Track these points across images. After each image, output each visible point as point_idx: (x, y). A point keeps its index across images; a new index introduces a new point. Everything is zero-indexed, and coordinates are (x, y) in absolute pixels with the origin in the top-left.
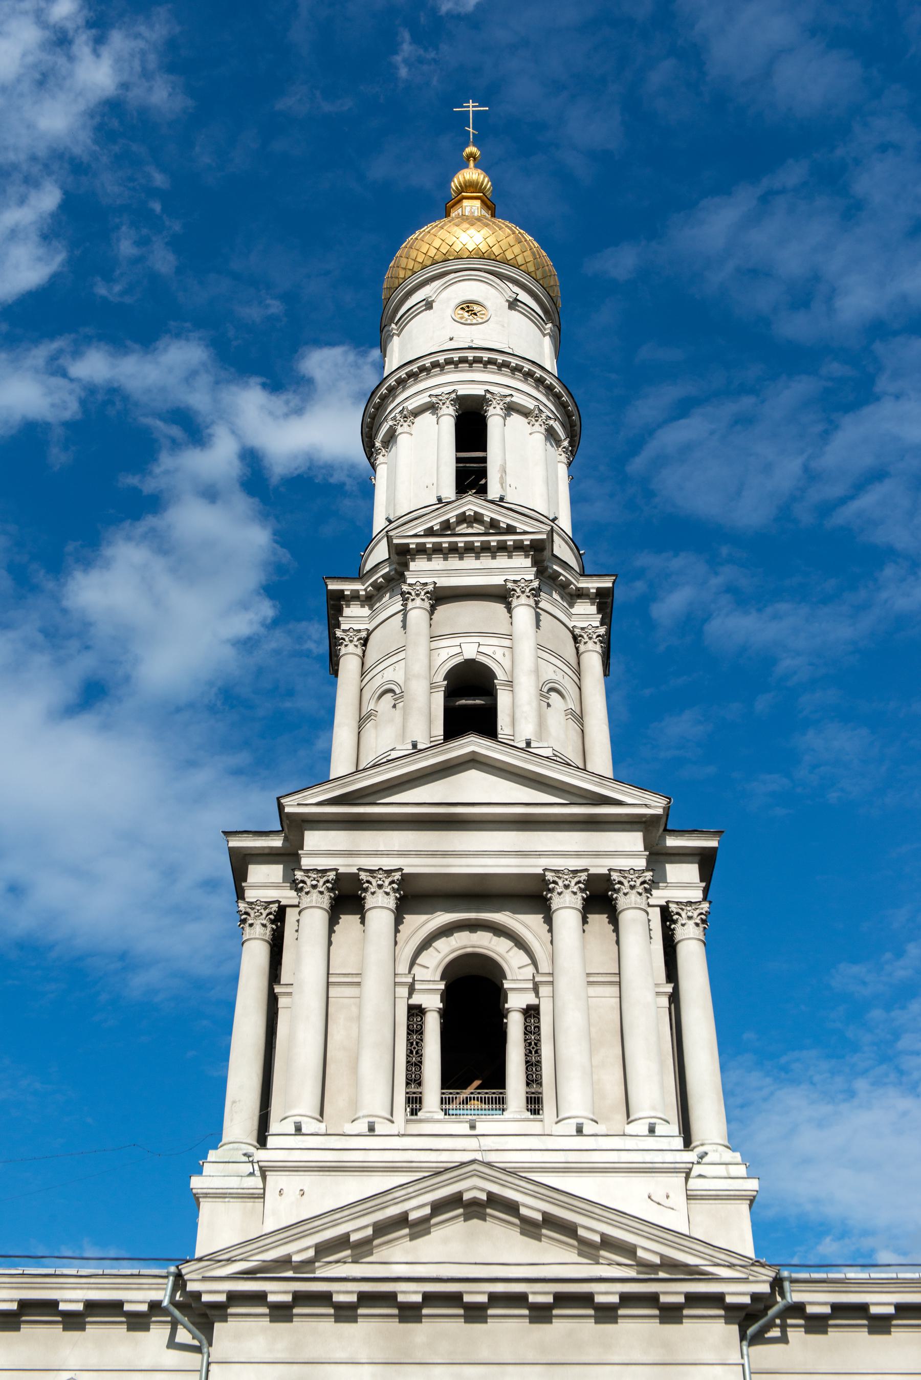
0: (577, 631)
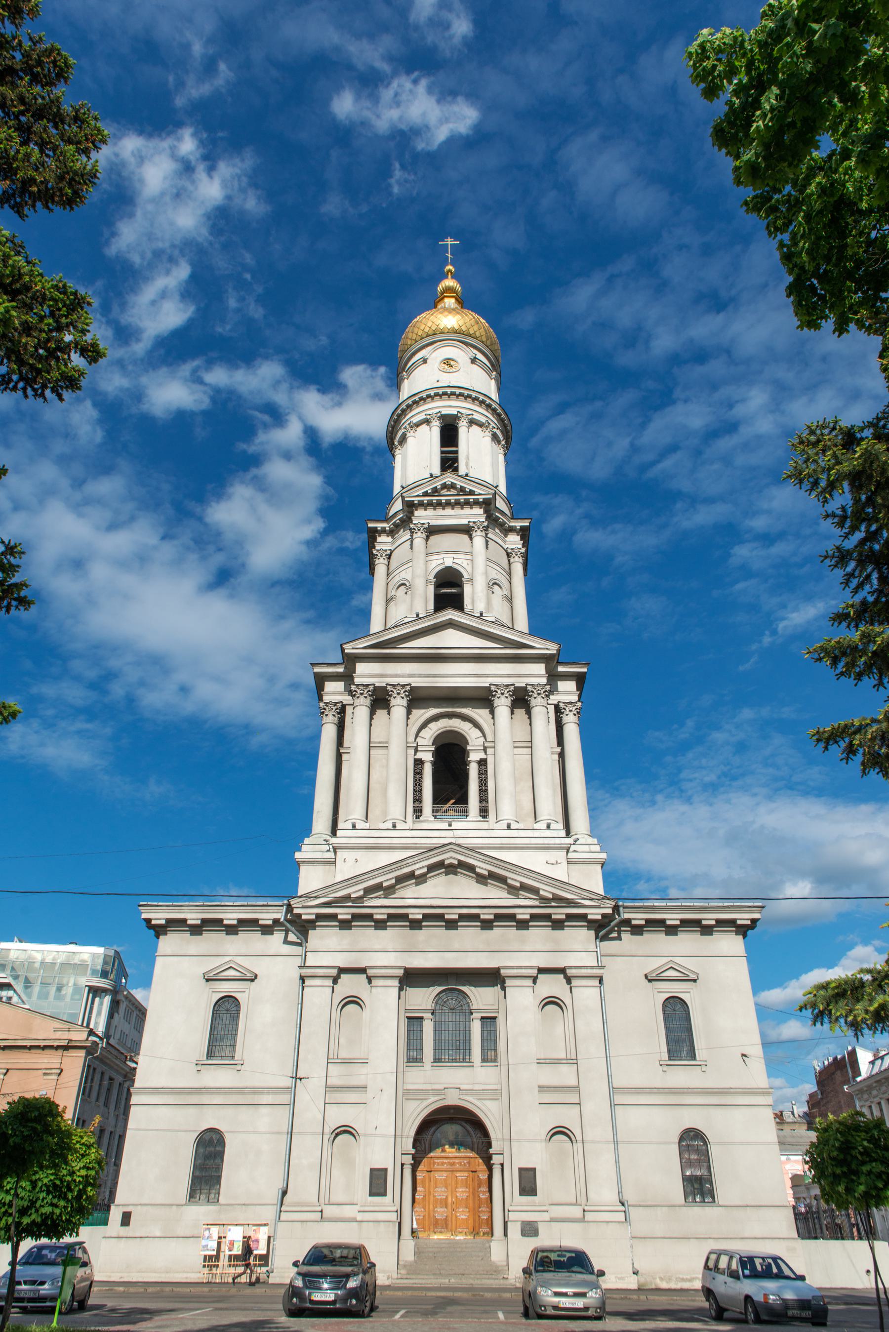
0: (509, 551)
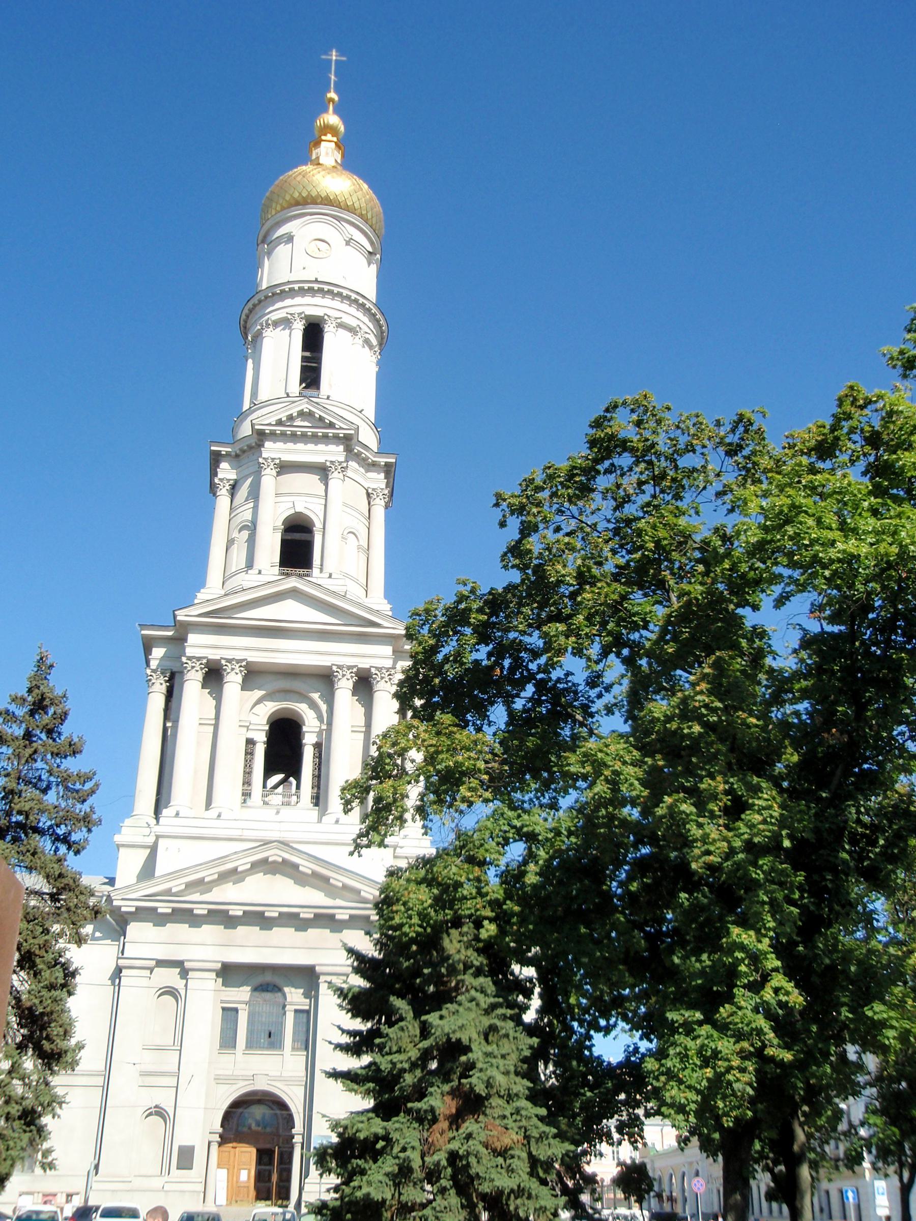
0: (370, 491)
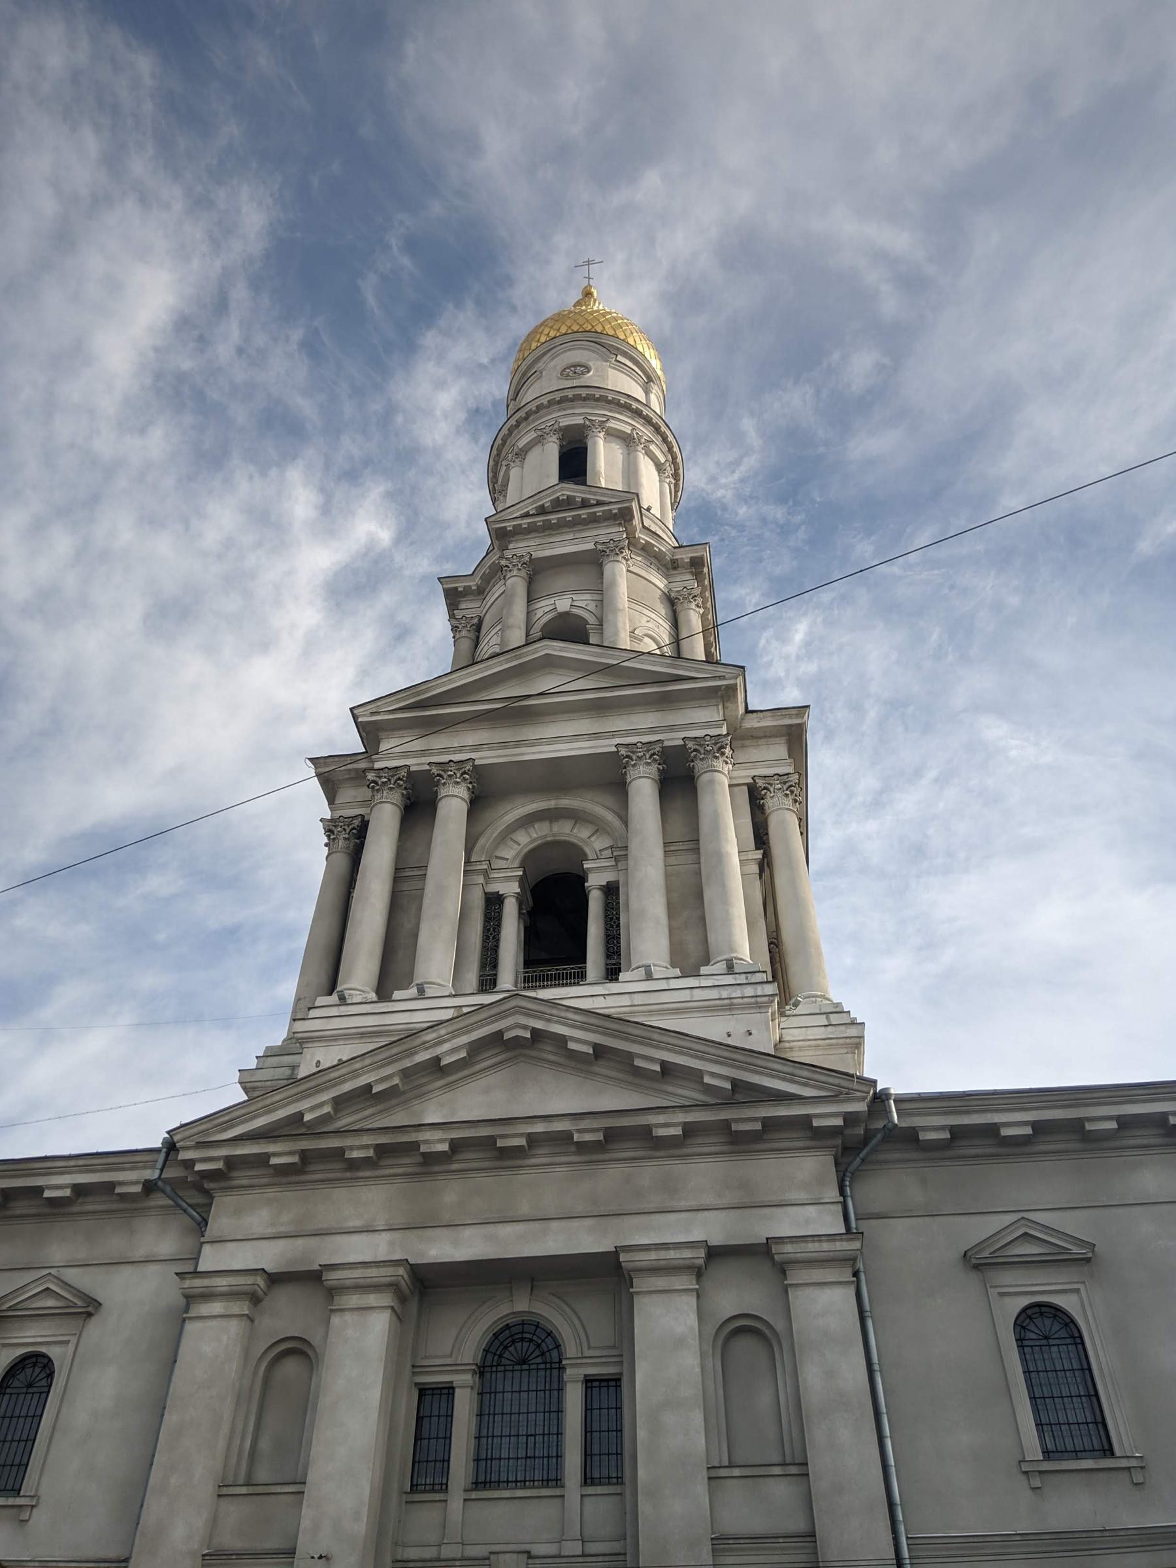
0: (673, 595)
